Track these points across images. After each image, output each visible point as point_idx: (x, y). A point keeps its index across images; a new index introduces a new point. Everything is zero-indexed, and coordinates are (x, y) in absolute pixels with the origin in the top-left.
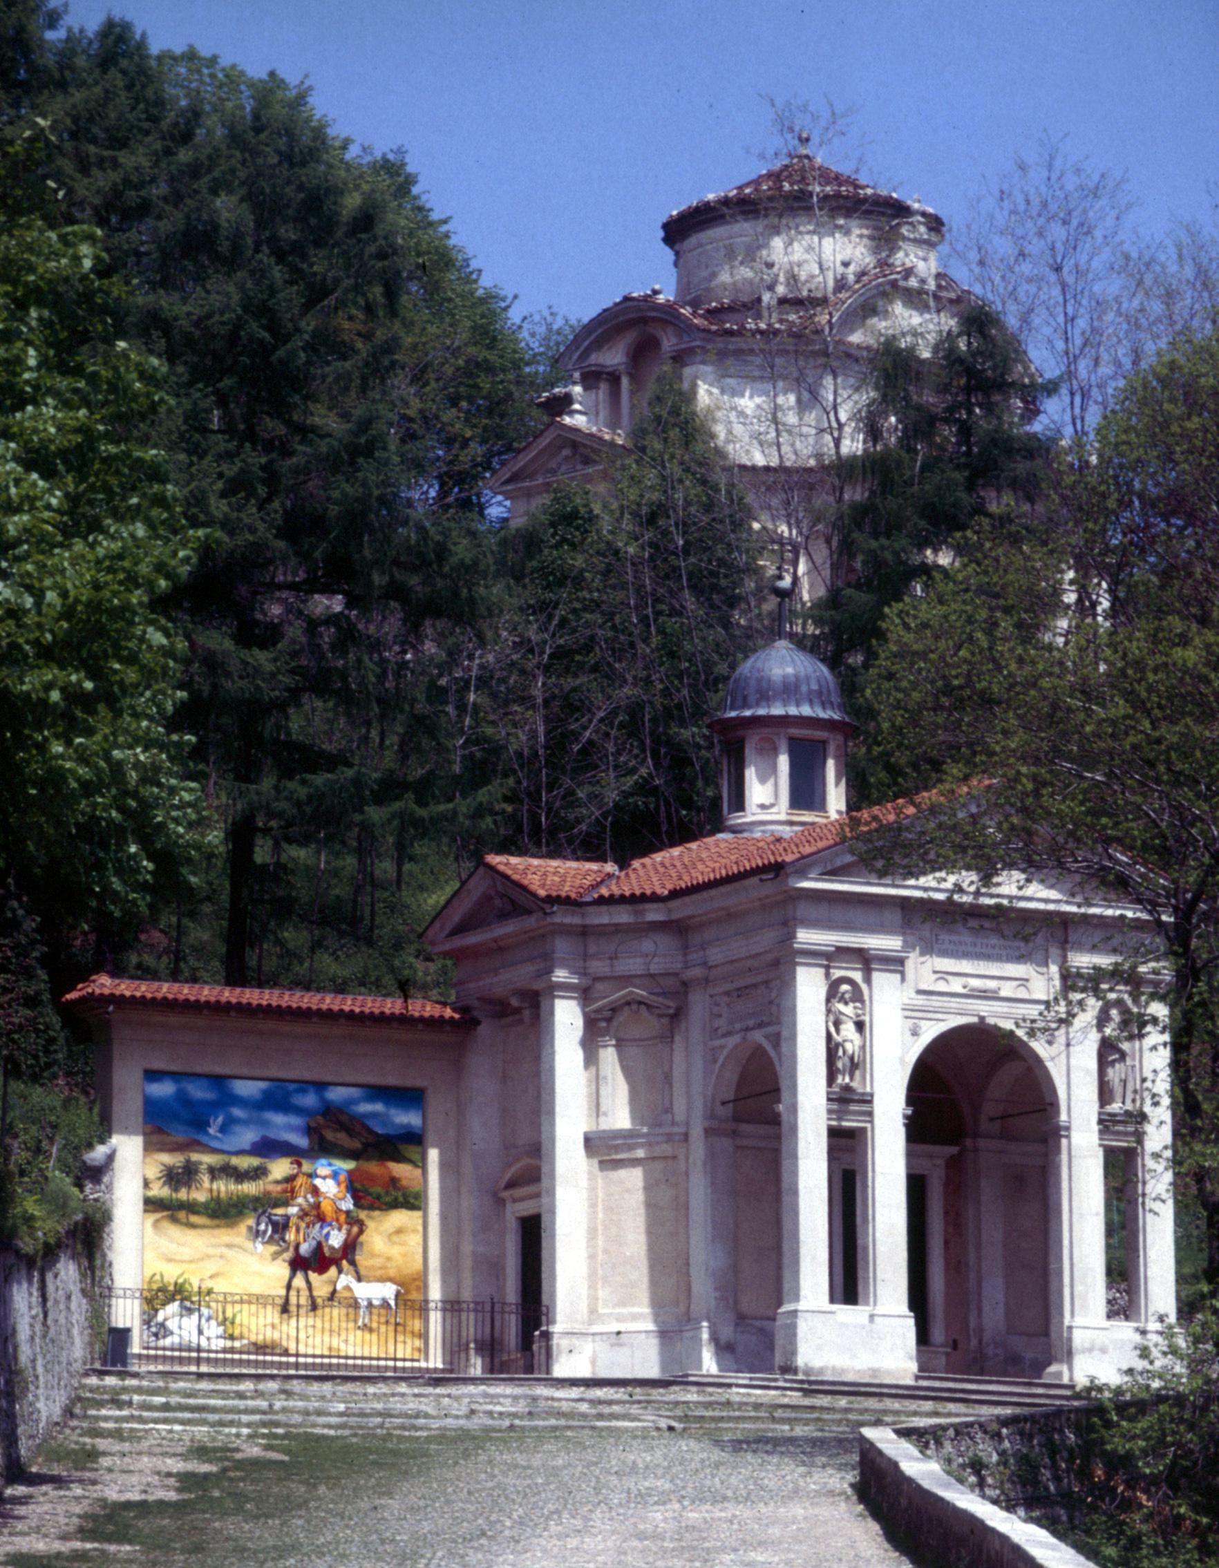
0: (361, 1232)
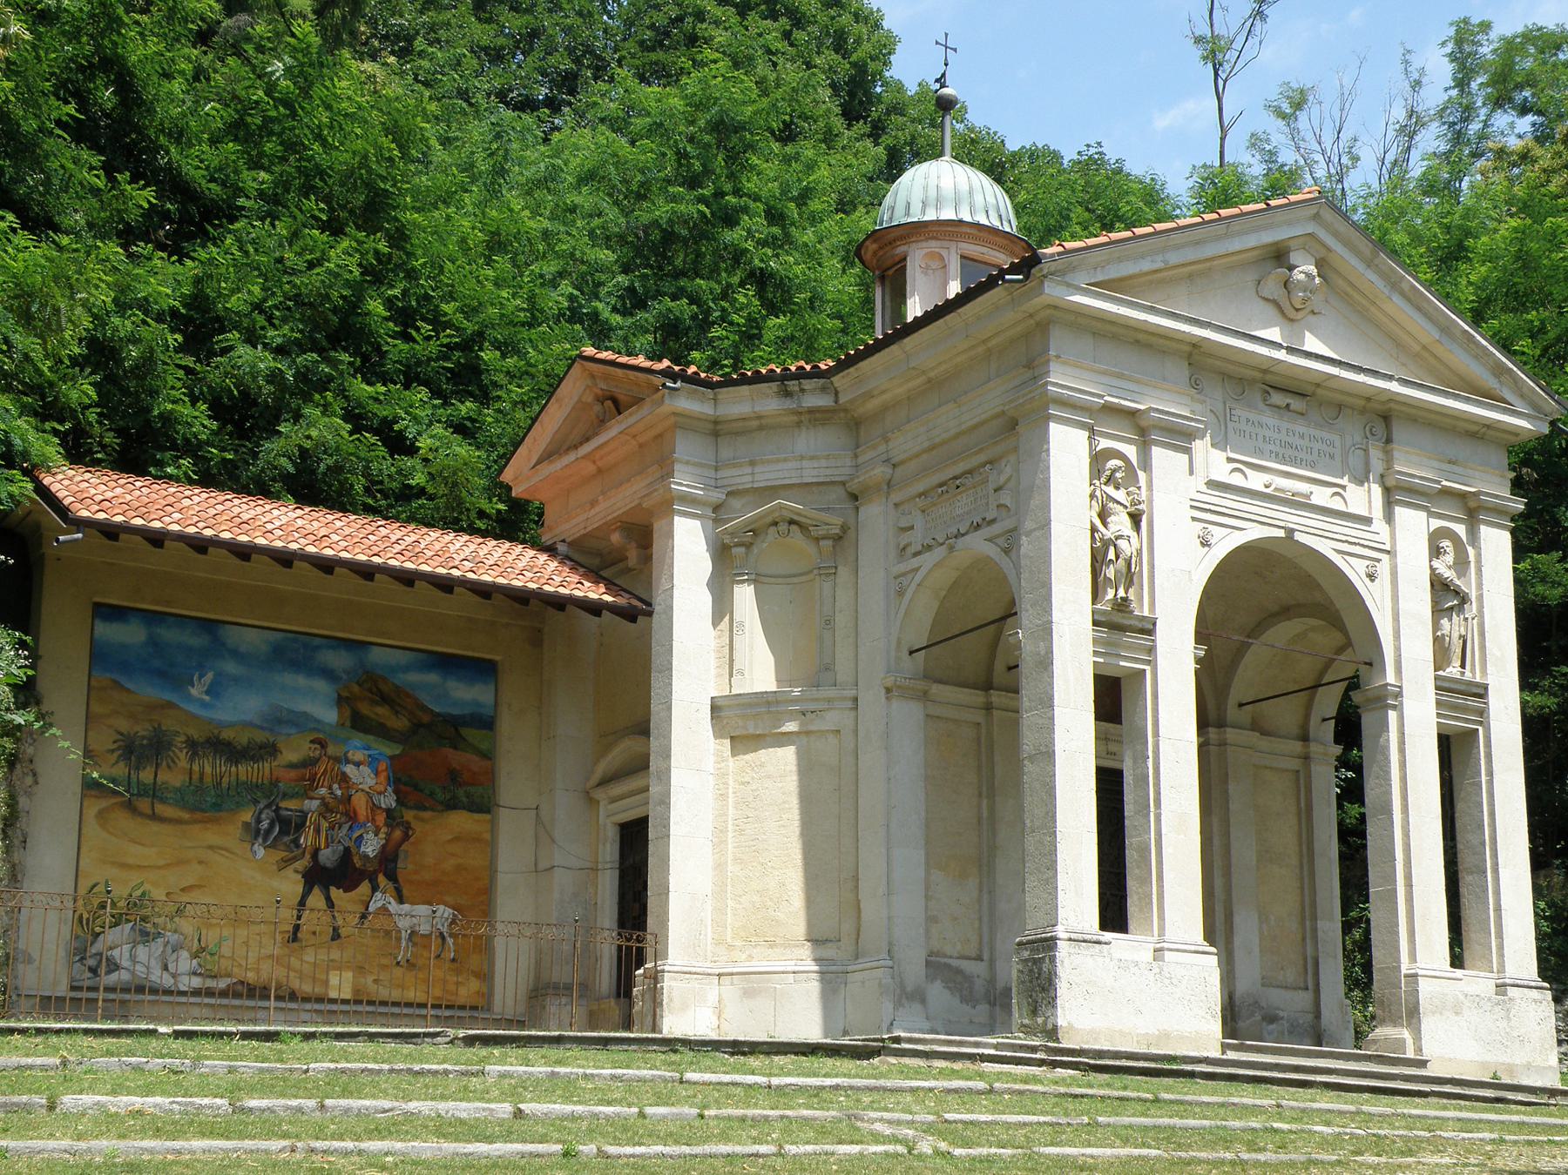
0: (406, 837)
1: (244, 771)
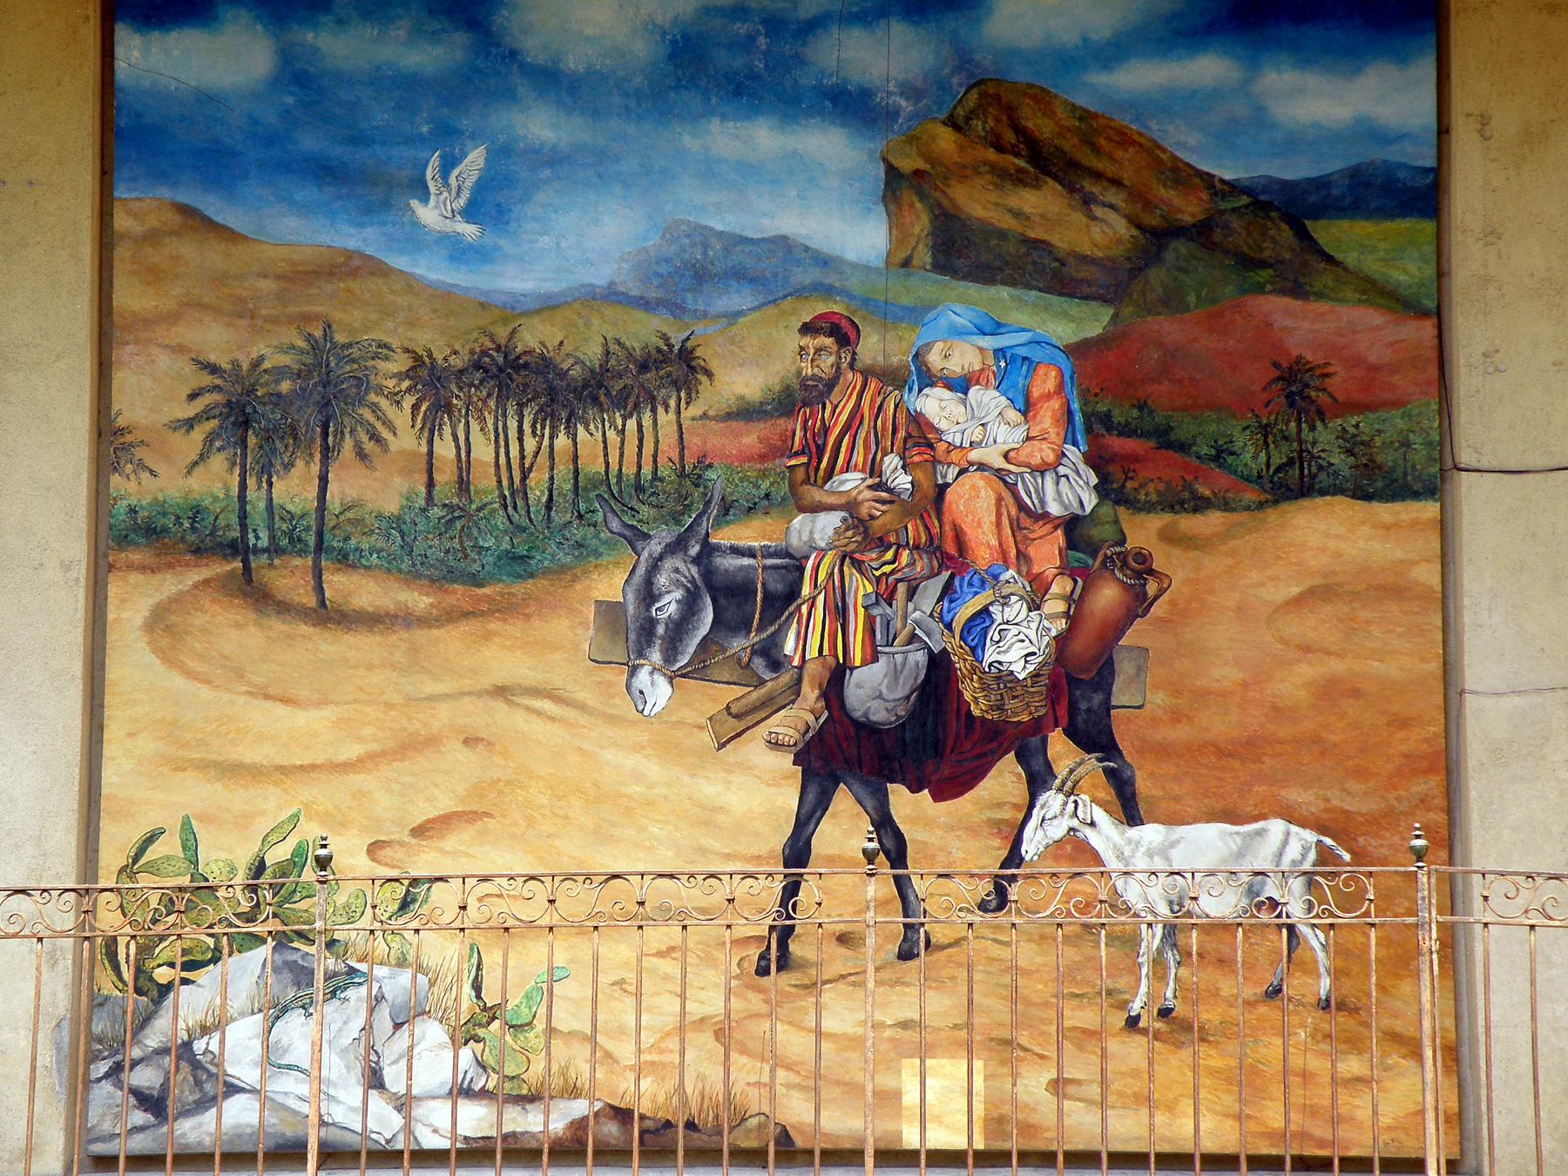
0: (1138, 604)
1: (596, 443)
